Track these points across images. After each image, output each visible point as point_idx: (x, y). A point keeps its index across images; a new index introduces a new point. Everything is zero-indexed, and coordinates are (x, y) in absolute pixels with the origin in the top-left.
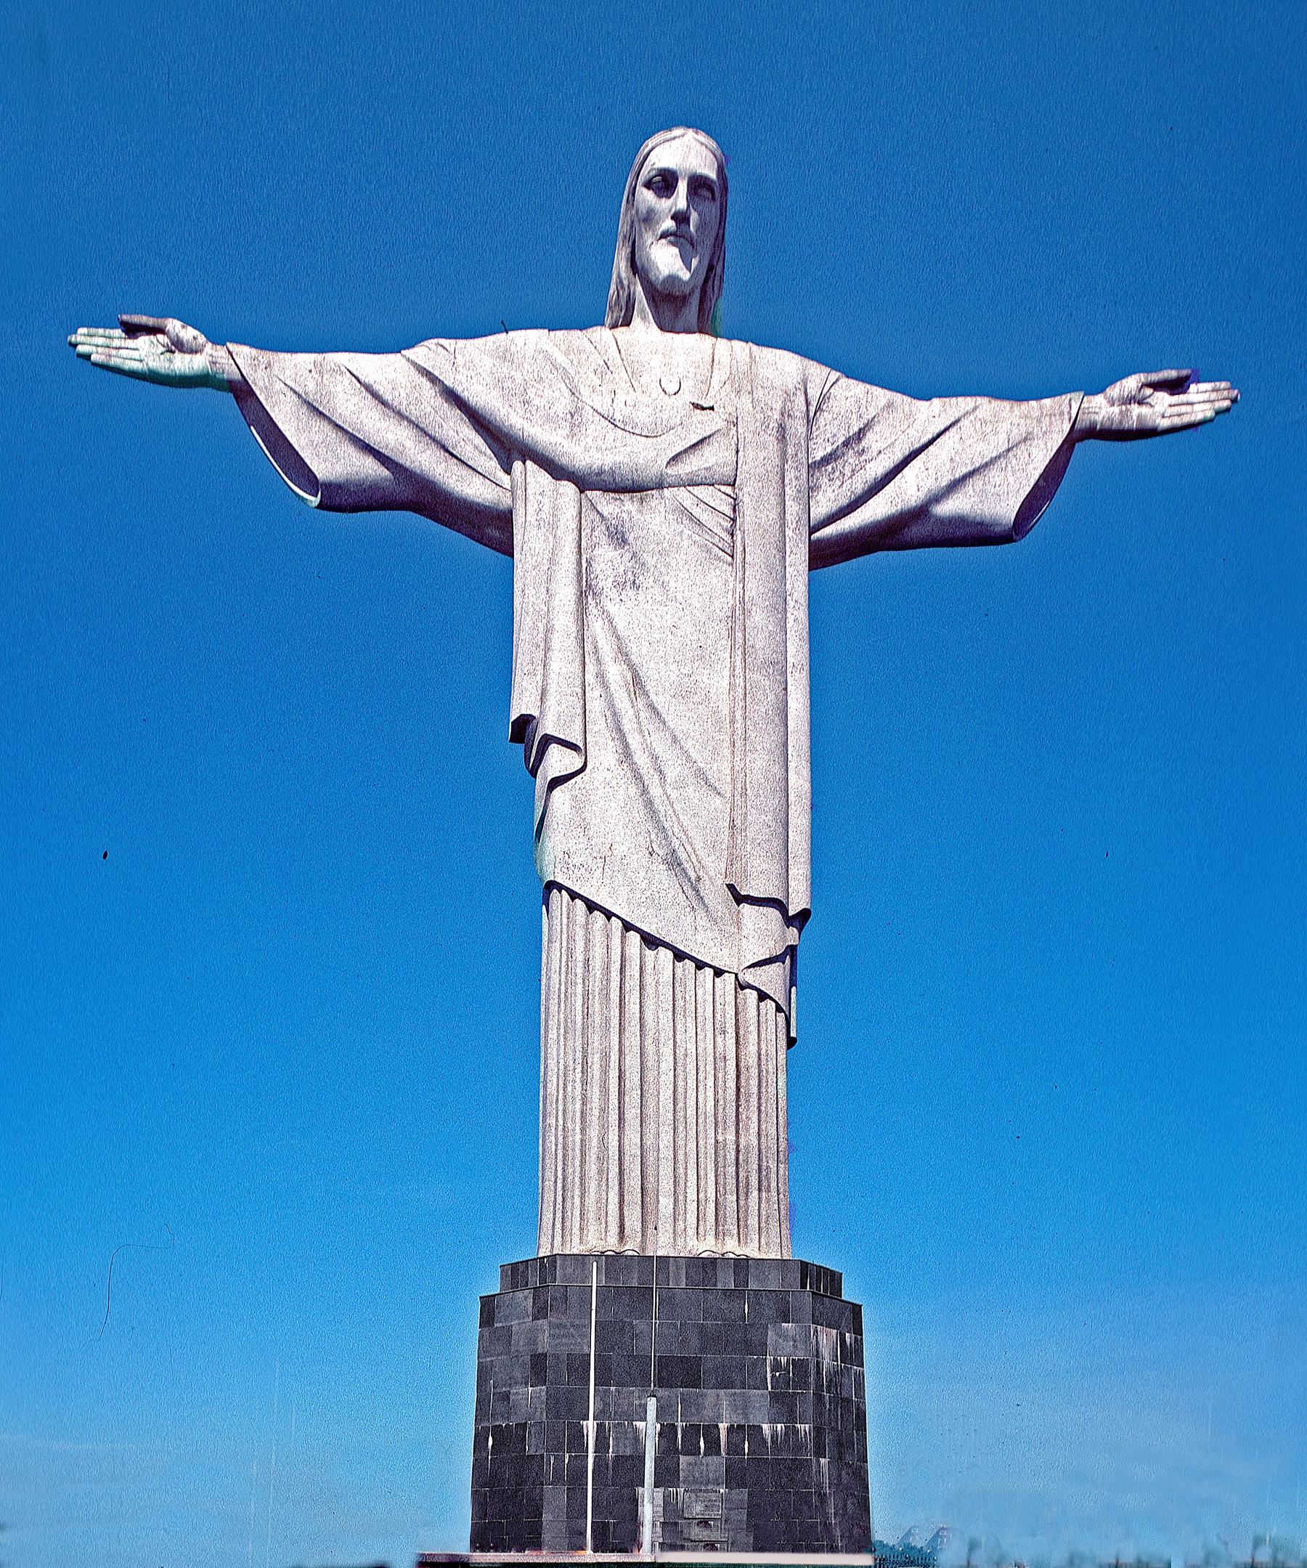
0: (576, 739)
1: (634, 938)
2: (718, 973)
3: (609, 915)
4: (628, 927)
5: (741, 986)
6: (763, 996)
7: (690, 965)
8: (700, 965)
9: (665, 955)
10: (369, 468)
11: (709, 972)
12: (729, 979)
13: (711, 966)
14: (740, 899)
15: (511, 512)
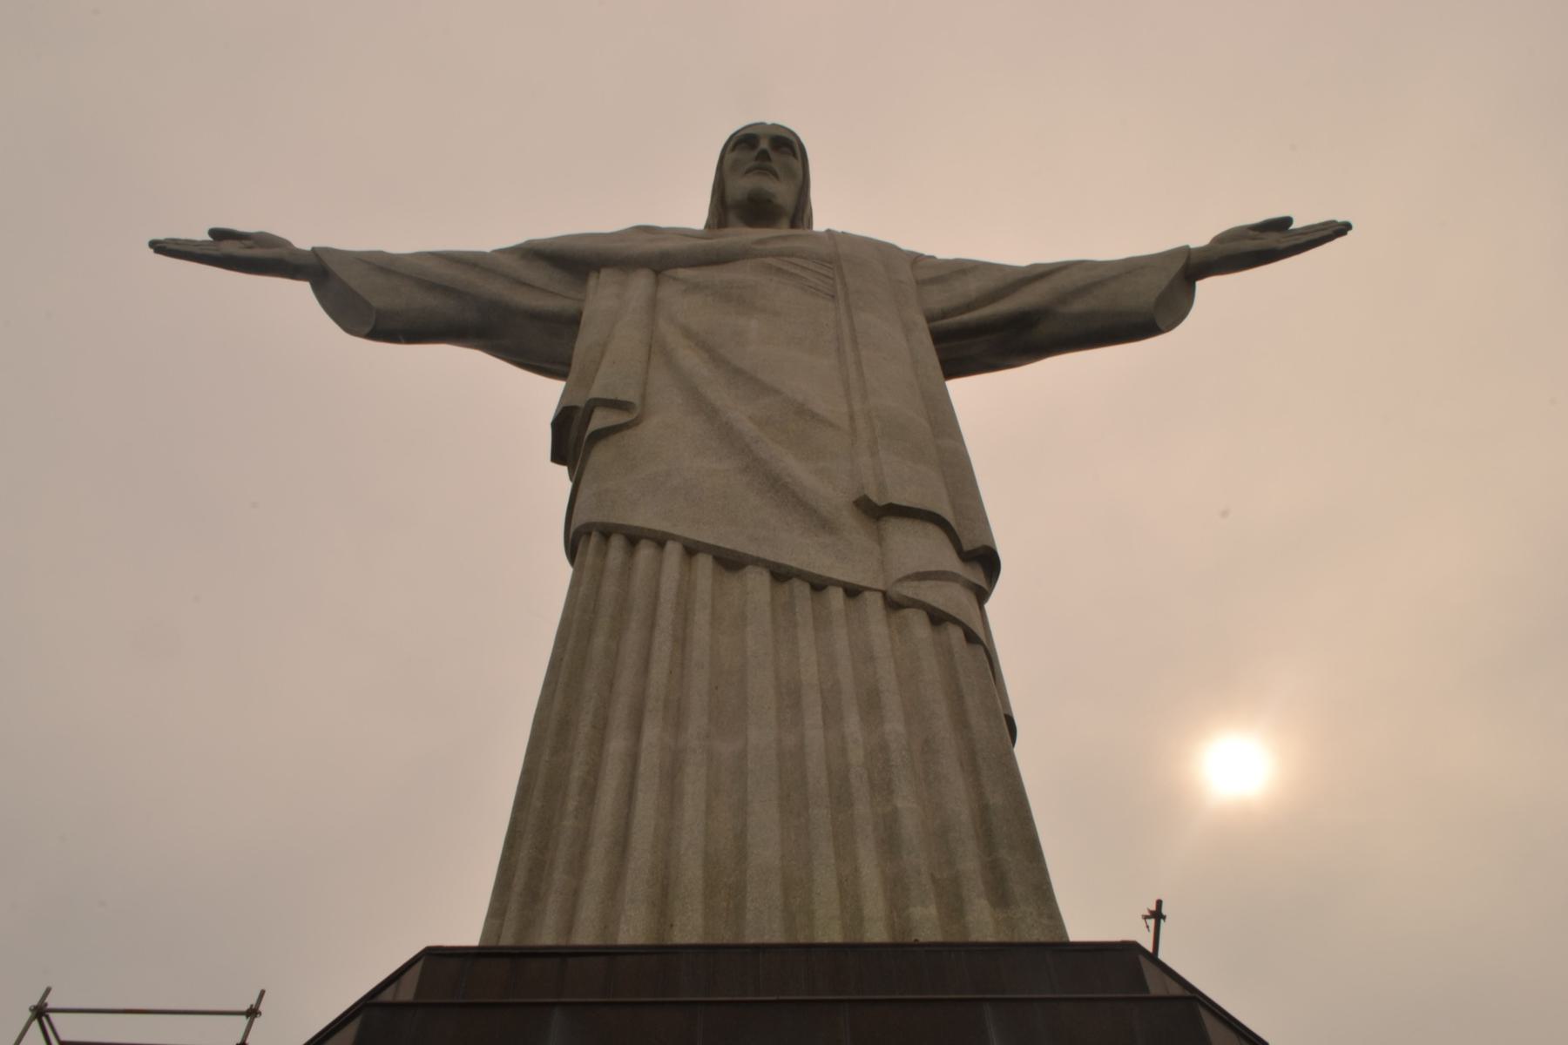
0: (630, 395)
1: (704, 563)
2: (852, 592)
3: (660, 540)
4: (691, 550)
5: (894, 605)
6: (938, 618)
7: (802, 589)
8: (819, 585)
9: (757, 583)
10: (432, 301)
11: (836, 597)
12: (874, 603)
13: (837, 583)
14: (876, 512)
15: (581, 313)
